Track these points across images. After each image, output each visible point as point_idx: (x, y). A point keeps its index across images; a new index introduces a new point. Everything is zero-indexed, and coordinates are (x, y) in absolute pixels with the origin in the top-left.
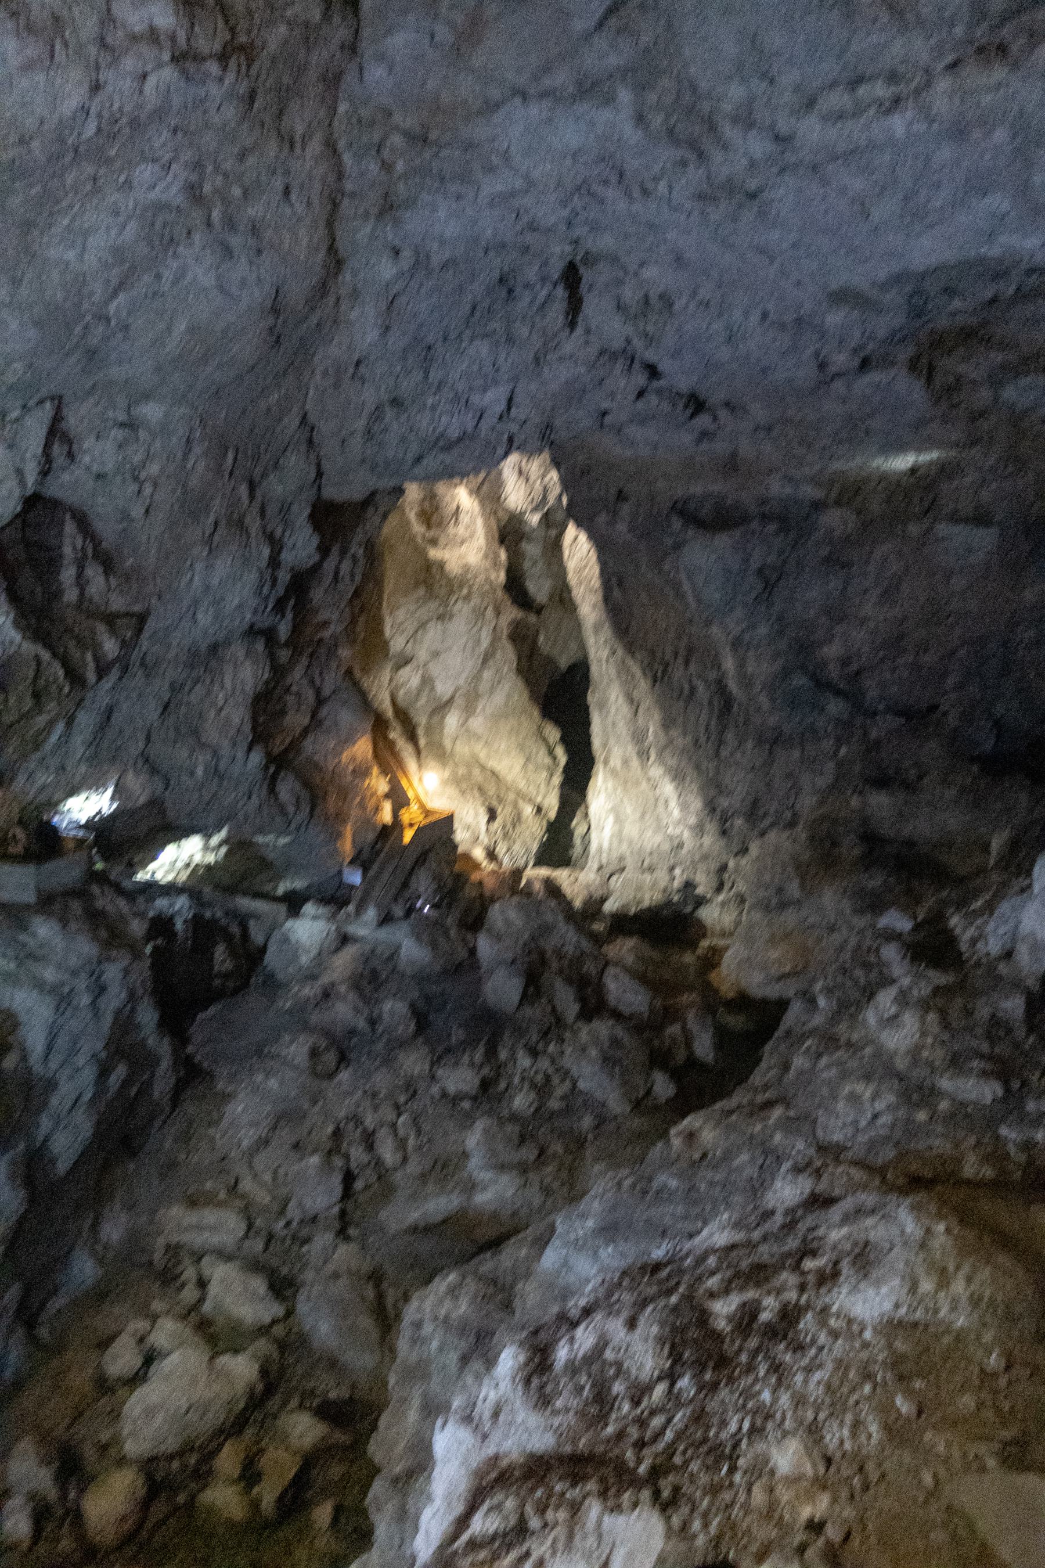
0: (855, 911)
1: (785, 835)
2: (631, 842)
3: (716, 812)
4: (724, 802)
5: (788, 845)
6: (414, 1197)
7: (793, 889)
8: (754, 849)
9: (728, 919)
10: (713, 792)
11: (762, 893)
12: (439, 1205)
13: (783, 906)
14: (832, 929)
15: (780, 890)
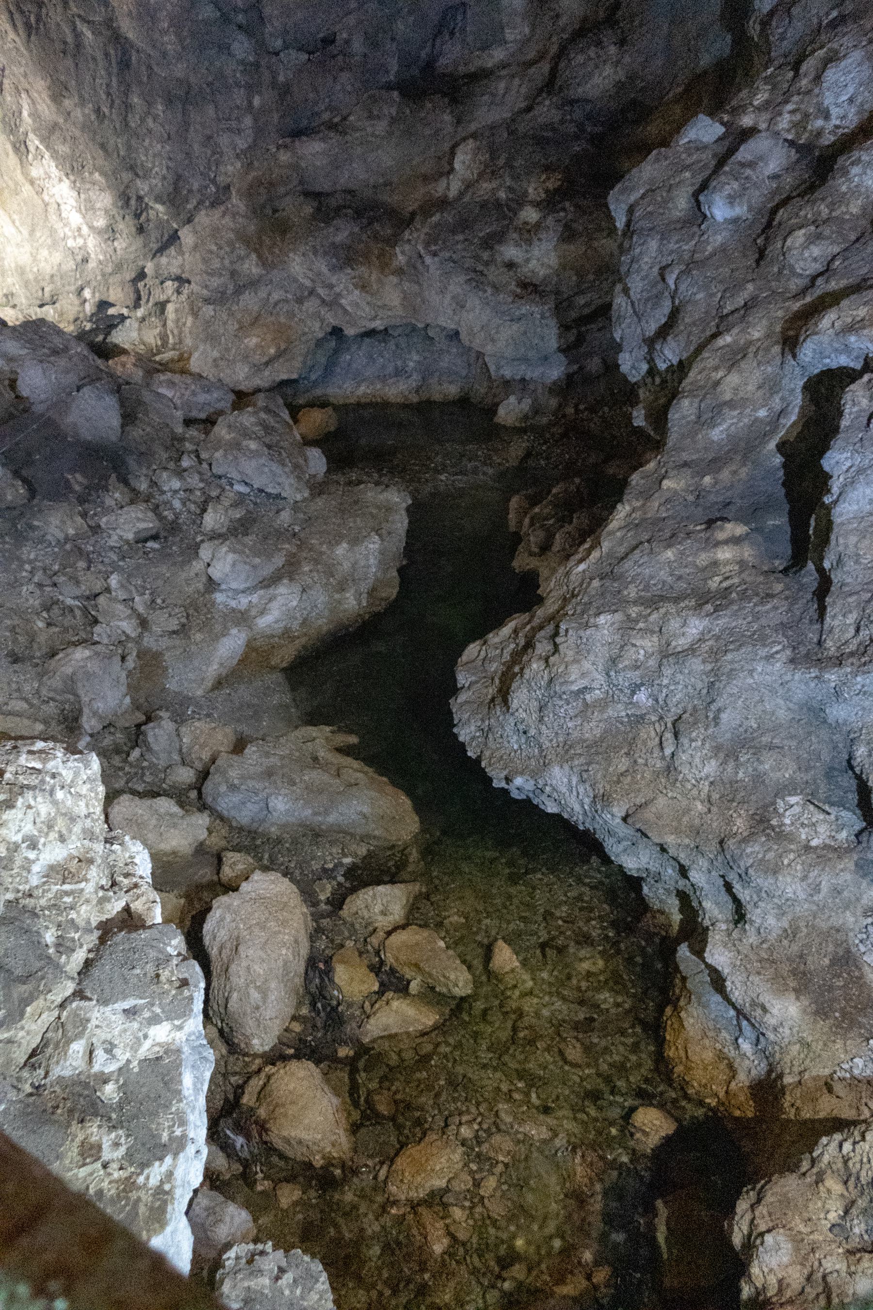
0: (333, 269)
1: (217, 212)
2: (21, 271)
3: (130, 204)
4: (143, 187)
5: (227, 220)
6: (187, 655)
7: (251, 267)
8: (187, 236)
9: (151, 337)
10: (126, 176)
11: (215, 282)
12: (231, 645)
13: (239, 291)
14: (300, 301)
15: (233, 274)
